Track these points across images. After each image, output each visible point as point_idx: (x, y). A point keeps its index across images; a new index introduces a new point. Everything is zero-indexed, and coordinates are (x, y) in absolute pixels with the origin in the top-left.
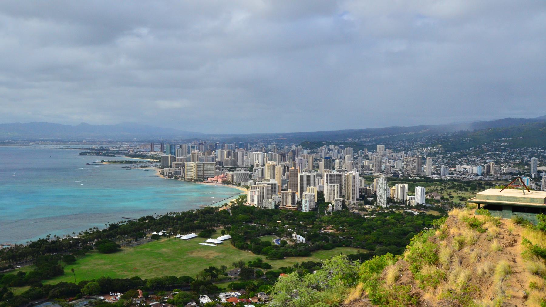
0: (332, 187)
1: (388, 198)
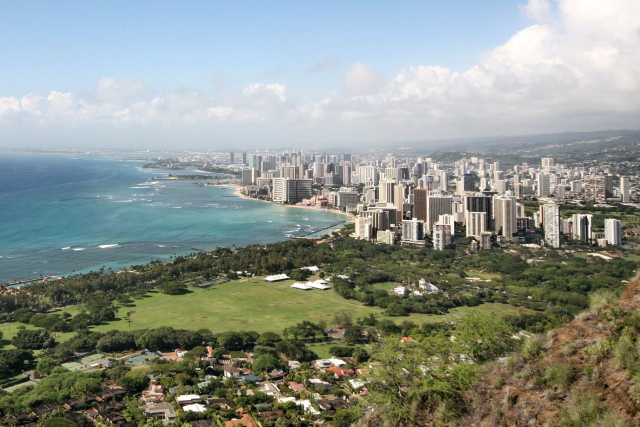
0: (477, 216)
1: (561, 233)
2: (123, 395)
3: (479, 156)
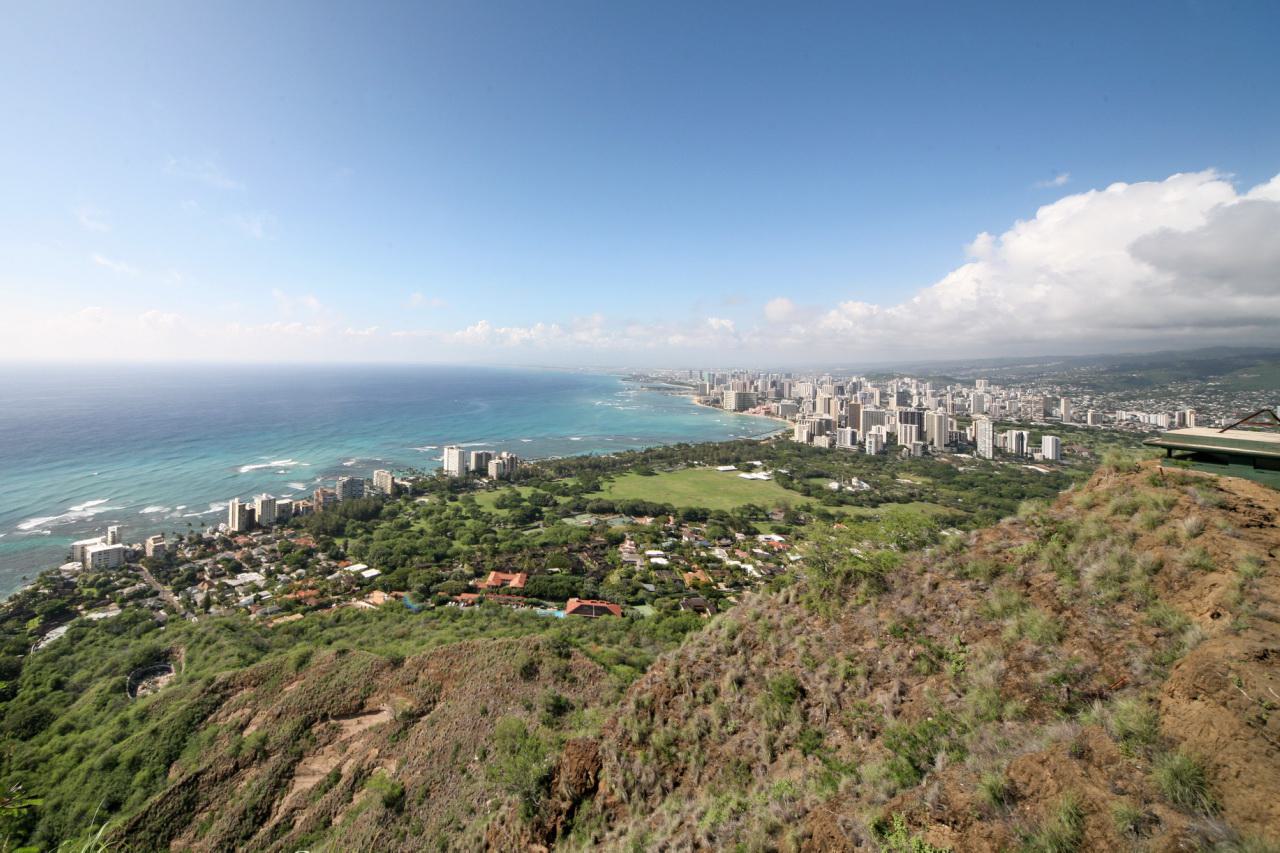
1: (994, 446)
2: (606, 545)
3: (912, 377)
